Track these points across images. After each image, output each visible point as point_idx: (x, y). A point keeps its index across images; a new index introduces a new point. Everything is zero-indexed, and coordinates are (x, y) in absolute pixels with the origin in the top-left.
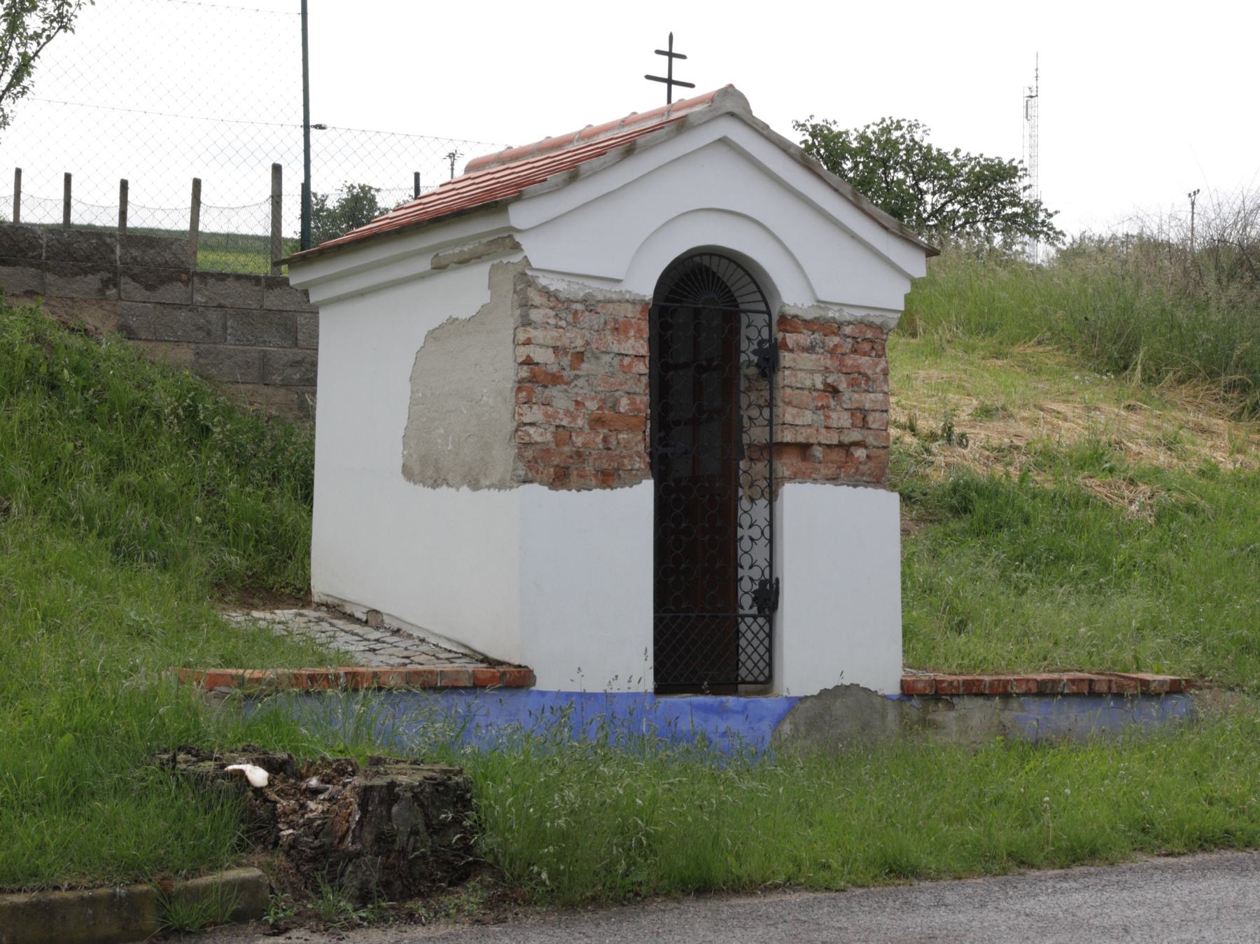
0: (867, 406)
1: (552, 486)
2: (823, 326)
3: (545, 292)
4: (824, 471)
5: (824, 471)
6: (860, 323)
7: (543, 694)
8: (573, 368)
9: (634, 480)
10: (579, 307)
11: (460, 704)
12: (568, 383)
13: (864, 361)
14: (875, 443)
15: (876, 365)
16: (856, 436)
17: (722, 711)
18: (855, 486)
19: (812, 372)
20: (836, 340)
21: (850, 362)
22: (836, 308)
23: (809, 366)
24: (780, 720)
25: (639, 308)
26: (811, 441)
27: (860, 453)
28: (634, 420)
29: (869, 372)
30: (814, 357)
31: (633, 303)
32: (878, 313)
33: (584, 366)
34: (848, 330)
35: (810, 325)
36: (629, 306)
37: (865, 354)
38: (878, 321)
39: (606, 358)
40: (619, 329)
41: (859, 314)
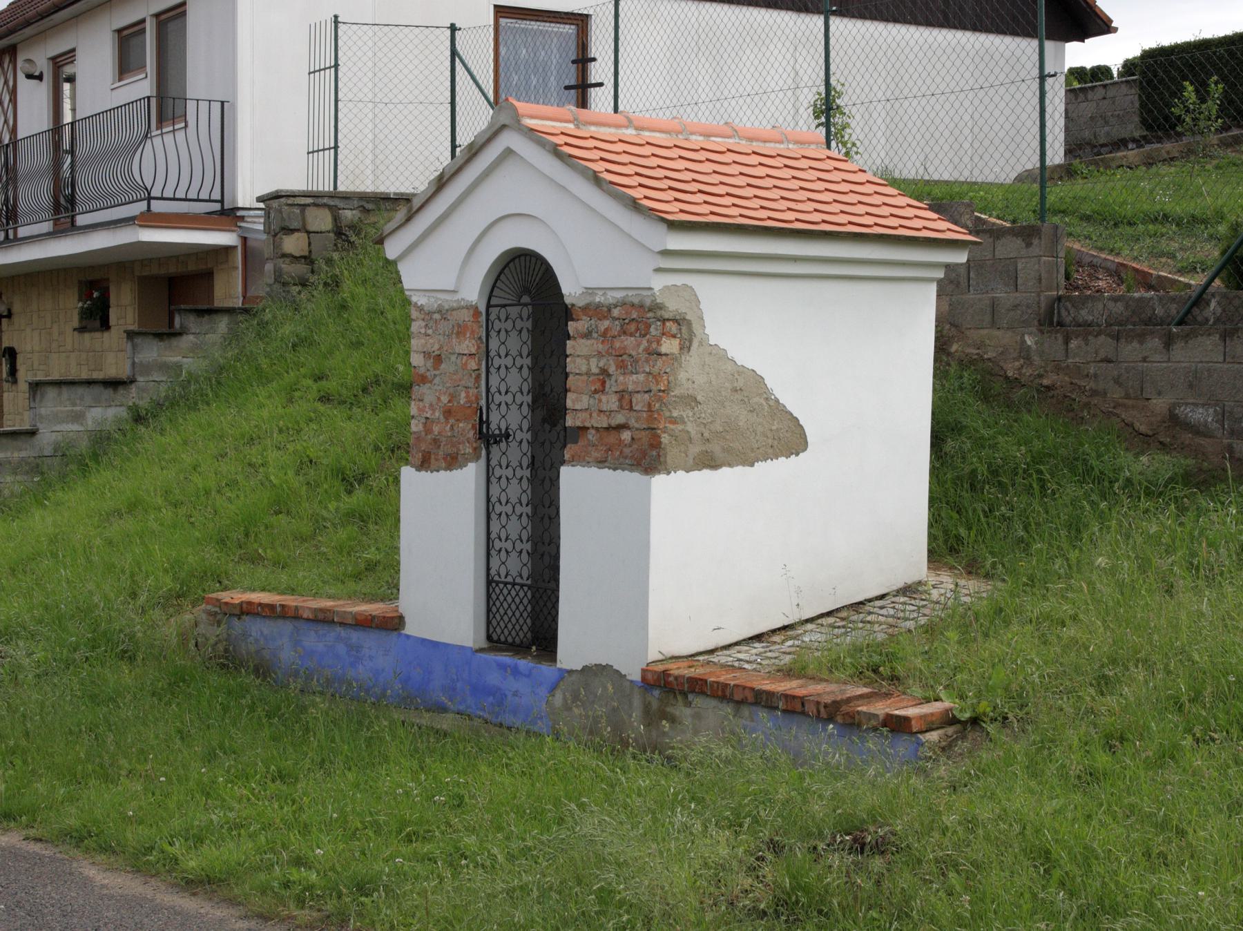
0: (631, 388)
1: (449, 467)
2: (597, 311)
3: (420, 309)
4: (596, 454)
5: (596, 454)
6: (622, 304)
7: (408, 637)
8: (436, 368)
9: (453, 462)
10: (437, 316)
11: (355, 636)
12: (431, 382)
13: (629, 341)
14: (637, 426)
15: (639, 345)
16: (619, 419)
17: (516, 672)
18: (615, 469)
19: (587, 358)
20: (606, 323)
21: (617, 345)
22: (600, 293)
23: (585, 351)
24: (553, 689)
25: (472, 312)
26: (587, 424)
27: (626, 436)
28: (468, 411)
29: (634, 353)
30: (589, 342)
31: (467, 308)
32: (634, 293)
33: (443, 366)
34: (616, 312)
35: (586, 309)
36: (465, 311)
37: (631, 335)
38: (636, 301)
39: (453, 358)
40: (460, 331)
41: (619, 295)
